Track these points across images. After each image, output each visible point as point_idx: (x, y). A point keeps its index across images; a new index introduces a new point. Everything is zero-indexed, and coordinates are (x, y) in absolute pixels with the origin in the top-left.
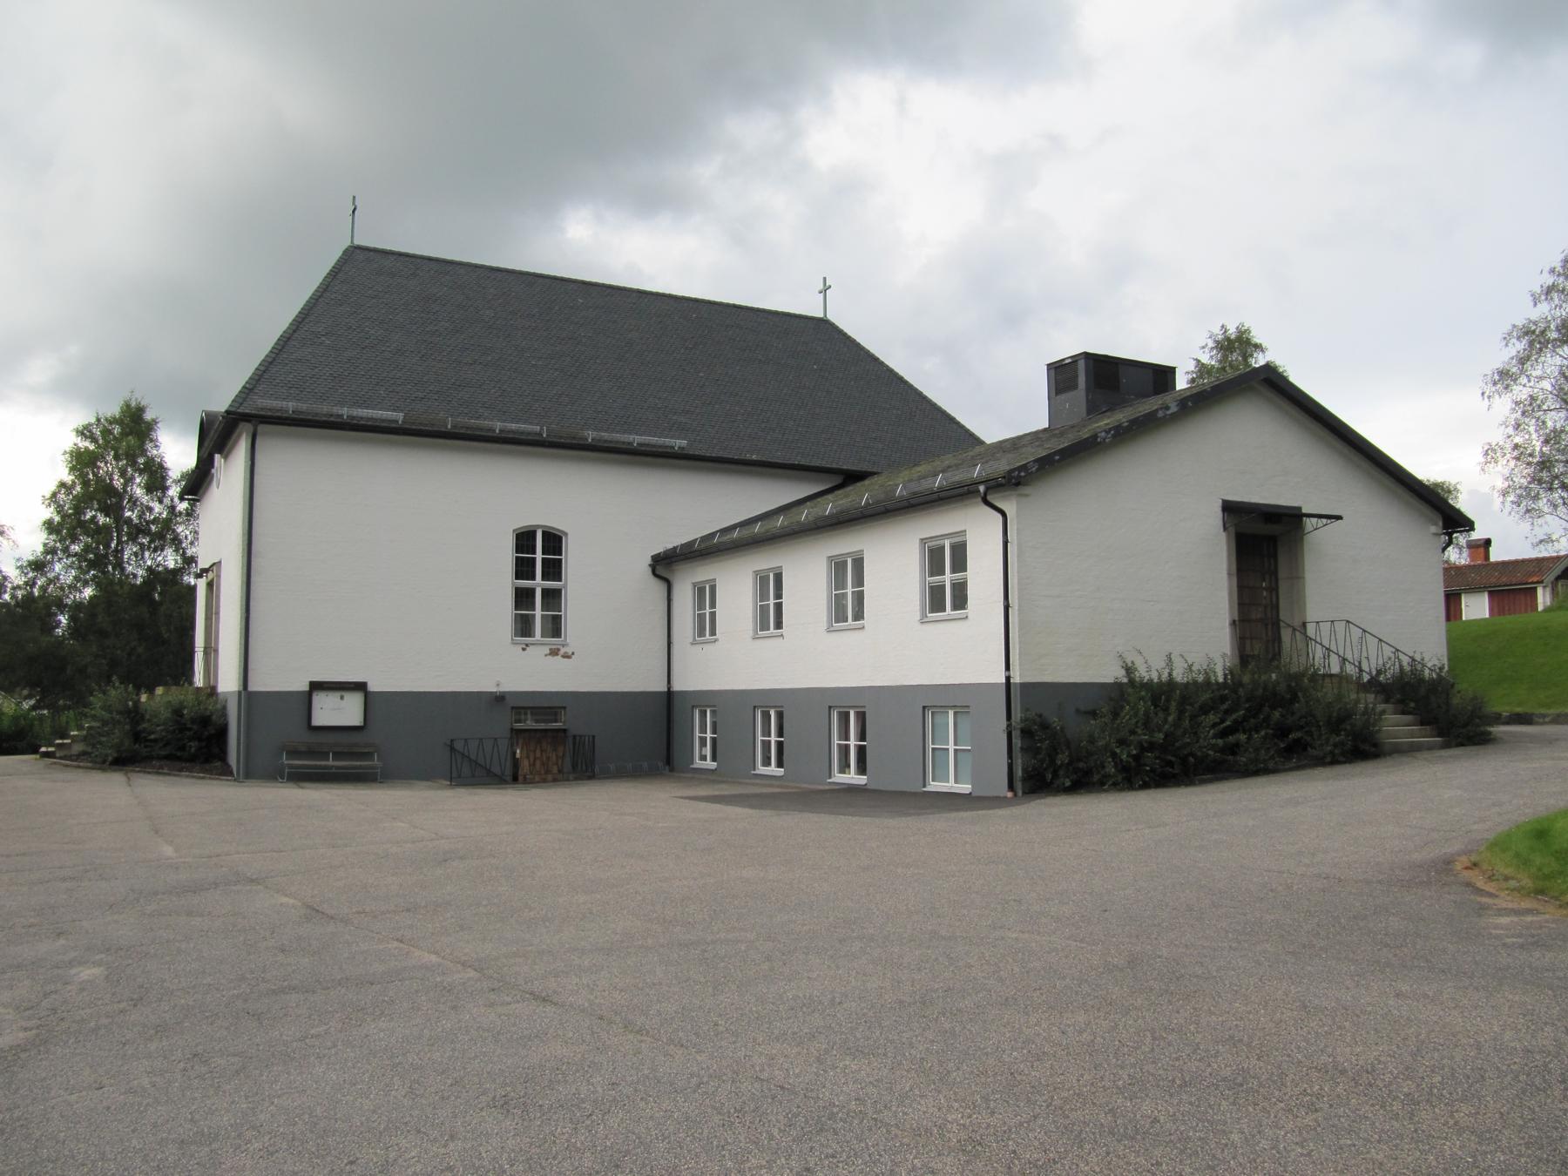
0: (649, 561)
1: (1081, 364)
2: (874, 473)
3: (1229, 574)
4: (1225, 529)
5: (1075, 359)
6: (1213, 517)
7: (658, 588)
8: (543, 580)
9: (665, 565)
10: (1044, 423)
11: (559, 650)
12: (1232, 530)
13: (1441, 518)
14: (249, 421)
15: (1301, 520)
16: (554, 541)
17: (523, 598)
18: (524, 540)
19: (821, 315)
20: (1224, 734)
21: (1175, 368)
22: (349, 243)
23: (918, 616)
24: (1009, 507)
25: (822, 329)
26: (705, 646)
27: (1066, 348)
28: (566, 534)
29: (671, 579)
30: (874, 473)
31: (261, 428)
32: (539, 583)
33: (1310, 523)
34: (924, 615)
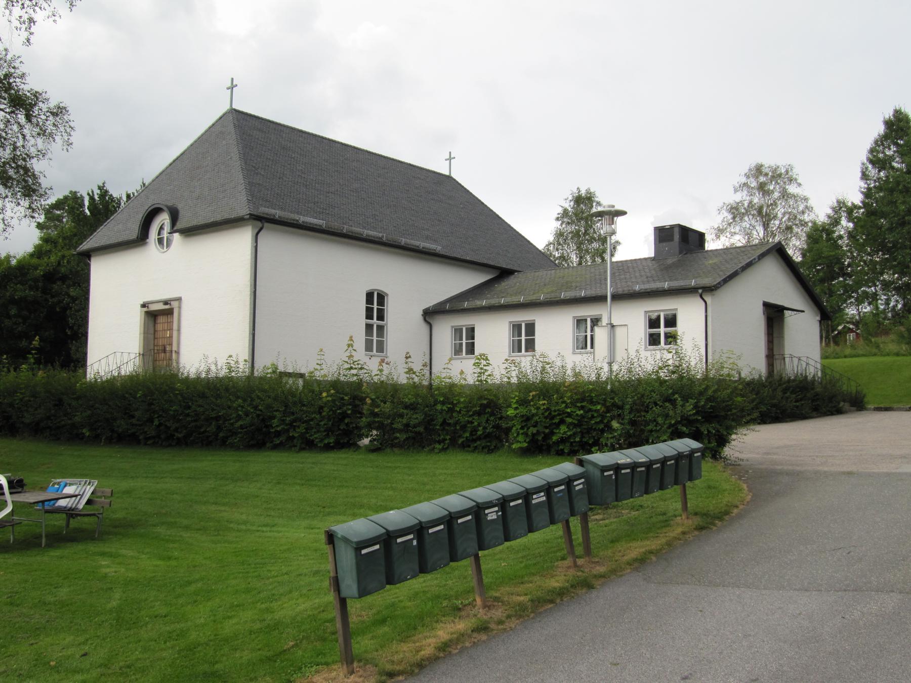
0: (421, 313)
1: (676, 230)
2: (520, 271)
3: (765, 334)
4: (764, 314)
5: (672, 227)
6: (760, 308)
7: (424, 328)
8: (377, 320)
9: (430, 315)
10: (653, 255)
11: (384, 359)
12: (766, 314)
13: (819, 315)
14: (261, 221)
15: (783, 314)
16: (382, 298)
17: (369, 327)
18: (369, 296)
19: (447, 174)
20: (796, 401)
21: (656, 229)
22: (227, 107)
23: (571, 351)
24: (708, 299)
25: (447, 181)
26: (463, 361)
27: (668, 221)
28: (387, 295)
29: (431, 322)
30: (520, 271)
31: (266, 225)
32: (375, 321)
33: (787, 313)
34: (574, 350)
